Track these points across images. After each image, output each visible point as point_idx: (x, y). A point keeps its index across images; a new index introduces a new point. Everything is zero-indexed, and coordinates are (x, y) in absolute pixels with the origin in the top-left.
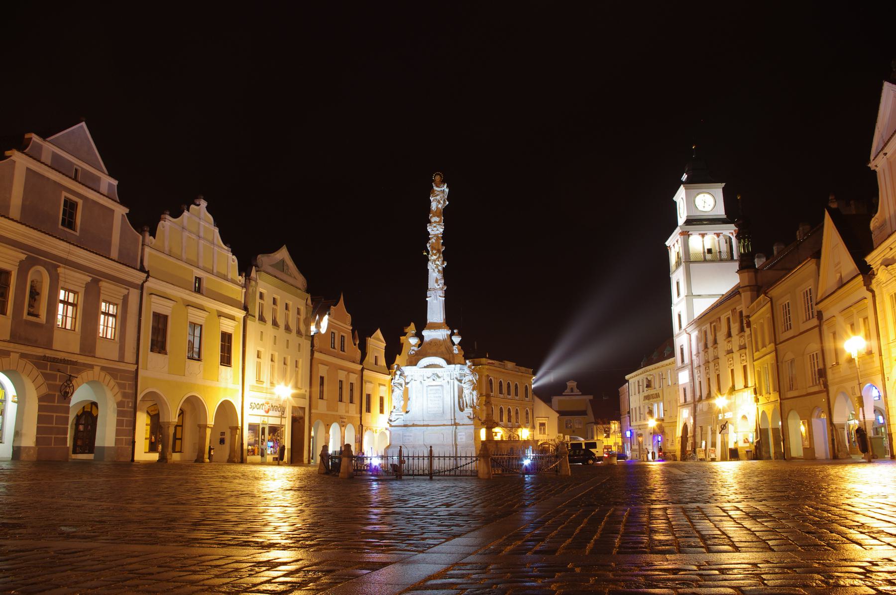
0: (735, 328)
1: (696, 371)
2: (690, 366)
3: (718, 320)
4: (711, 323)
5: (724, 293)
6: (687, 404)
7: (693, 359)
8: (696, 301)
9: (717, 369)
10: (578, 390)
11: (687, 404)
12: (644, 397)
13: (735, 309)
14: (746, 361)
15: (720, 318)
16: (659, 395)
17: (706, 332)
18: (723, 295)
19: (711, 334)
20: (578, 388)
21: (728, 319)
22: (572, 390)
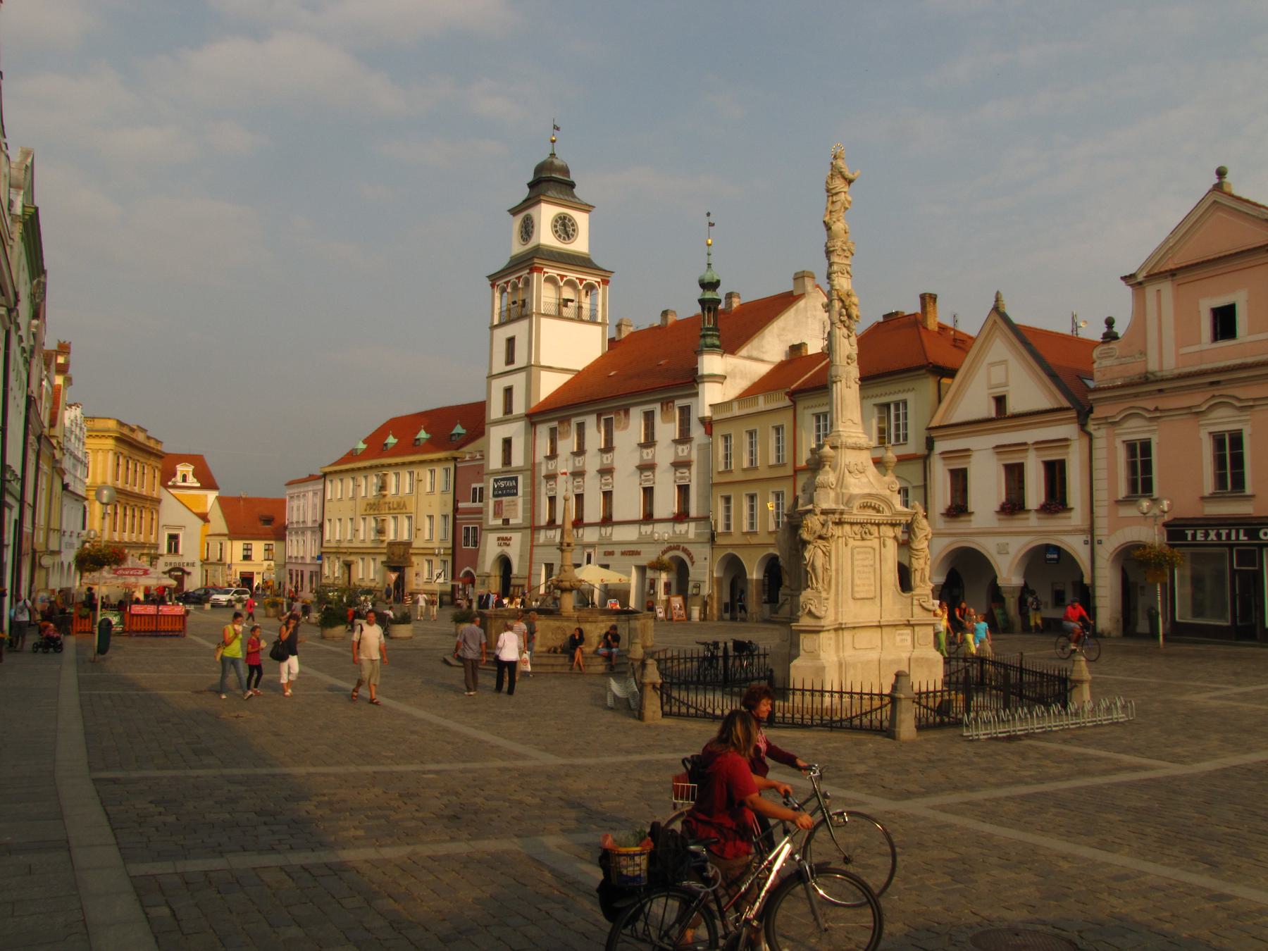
0: (667, 430)
1: (544, 482)
2: (529, 473)
3: (622, 413)
4: (599, 416)
5: (580, 368)
6: (511, 529)
7: (537, 461)
8: (544, 374)
9: (606, 485)
10: (195, 480)
11: (511, 529)
12: (368, 505)
13: (673, 402)
14: (690, 481)
15: (627, 412)
16: (404, 505)
17: (581, 427)
18: (578, 371)
19: (599, 431)
20: (195, 475)
21: (649, 417)
22: (184, 478)
